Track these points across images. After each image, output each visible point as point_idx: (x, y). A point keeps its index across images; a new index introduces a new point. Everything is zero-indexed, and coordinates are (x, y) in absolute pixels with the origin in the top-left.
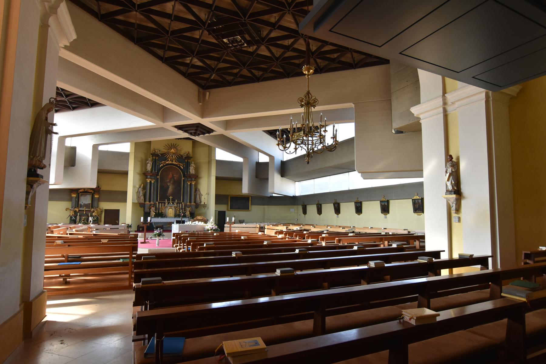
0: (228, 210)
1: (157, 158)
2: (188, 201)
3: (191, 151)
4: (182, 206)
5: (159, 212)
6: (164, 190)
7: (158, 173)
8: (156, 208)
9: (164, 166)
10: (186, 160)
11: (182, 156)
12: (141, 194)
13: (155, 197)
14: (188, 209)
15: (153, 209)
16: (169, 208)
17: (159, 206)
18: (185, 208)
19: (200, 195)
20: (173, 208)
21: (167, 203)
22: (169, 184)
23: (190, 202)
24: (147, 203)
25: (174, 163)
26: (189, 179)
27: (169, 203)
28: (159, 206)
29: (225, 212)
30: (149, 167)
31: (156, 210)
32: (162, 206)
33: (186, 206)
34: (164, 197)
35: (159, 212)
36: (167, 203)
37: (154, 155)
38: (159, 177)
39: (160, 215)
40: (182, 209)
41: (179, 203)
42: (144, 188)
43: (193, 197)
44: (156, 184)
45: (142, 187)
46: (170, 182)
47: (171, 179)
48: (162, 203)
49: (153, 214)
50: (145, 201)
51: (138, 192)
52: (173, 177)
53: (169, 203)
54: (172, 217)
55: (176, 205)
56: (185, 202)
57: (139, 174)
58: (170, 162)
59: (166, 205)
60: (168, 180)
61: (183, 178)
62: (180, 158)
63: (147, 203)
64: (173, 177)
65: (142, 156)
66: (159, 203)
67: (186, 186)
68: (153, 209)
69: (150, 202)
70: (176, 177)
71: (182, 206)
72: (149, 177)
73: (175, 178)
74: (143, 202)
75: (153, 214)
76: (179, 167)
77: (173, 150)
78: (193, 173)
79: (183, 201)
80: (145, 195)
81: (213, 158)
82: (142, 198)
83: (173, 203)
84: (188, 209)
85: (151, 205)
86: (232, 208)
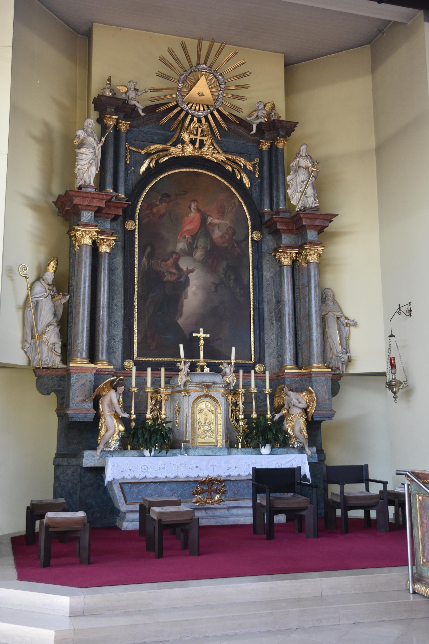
1: (124, 126)
2: (289, 356)
5: (141, 419)
6: (163, 294)
7: (133, 195)
8: (126, 395)
9: (159, 168)
10: (267, 140)
11: (245, 125)
12: (47, 315)
13: (119, 331)
14: (297, 401)
15: (112, 398)
16: (195, 392)
17: (141, 384)
18: (272, 396)
19: (345, 323)
22: (184, 264)
23: (297, 363)
24: (80, 362)
25: (208, 152)
26: (286, 239)
28: (141, 384)
30: (87, 167)
31: (126, 409)
32: (156, 383)
33: (278, 379)
34: (160, 337)
35: (141, 419)
36: (184, 368)
37: (108, 105)
38: (131, 225)
39: (151, 434)
40: (260, 397)
41: (247, 369)
42: (63, 285)
43: (316, 334)
44: (119, 260)
45: (49, 276)
46: (189, 252)
47: (194, 237)
48: (156, 367)
49: (112, 429)
50: (66, 354)
51: (29, 305)
52: (204, 227)
53: (193, 368)
54: (210, 449)
55: (230, 378)
56: (270, 360)
57: (35, 207)
58: (189, 150)
59: (182, 378)
60: (181, 245)
62: (231, 129)
63: (80, 362)
64: (204, 227)
65: (46, 112)
66: (141, 367)
67: (267, 274)
68: (112, 398)
69: (92, 357)
70: (220, 226)
72: (87, 216)
73: (217, 234)
74: (57, 361)
75: (112, 429)
76: (230, 177)
77: (202, 88)
78: (311, 202)
79: (260, 359)
80: (65, 324)
82: (52, 337)
83: (215, 369)
84: (297, 401)
85: (99, 376)
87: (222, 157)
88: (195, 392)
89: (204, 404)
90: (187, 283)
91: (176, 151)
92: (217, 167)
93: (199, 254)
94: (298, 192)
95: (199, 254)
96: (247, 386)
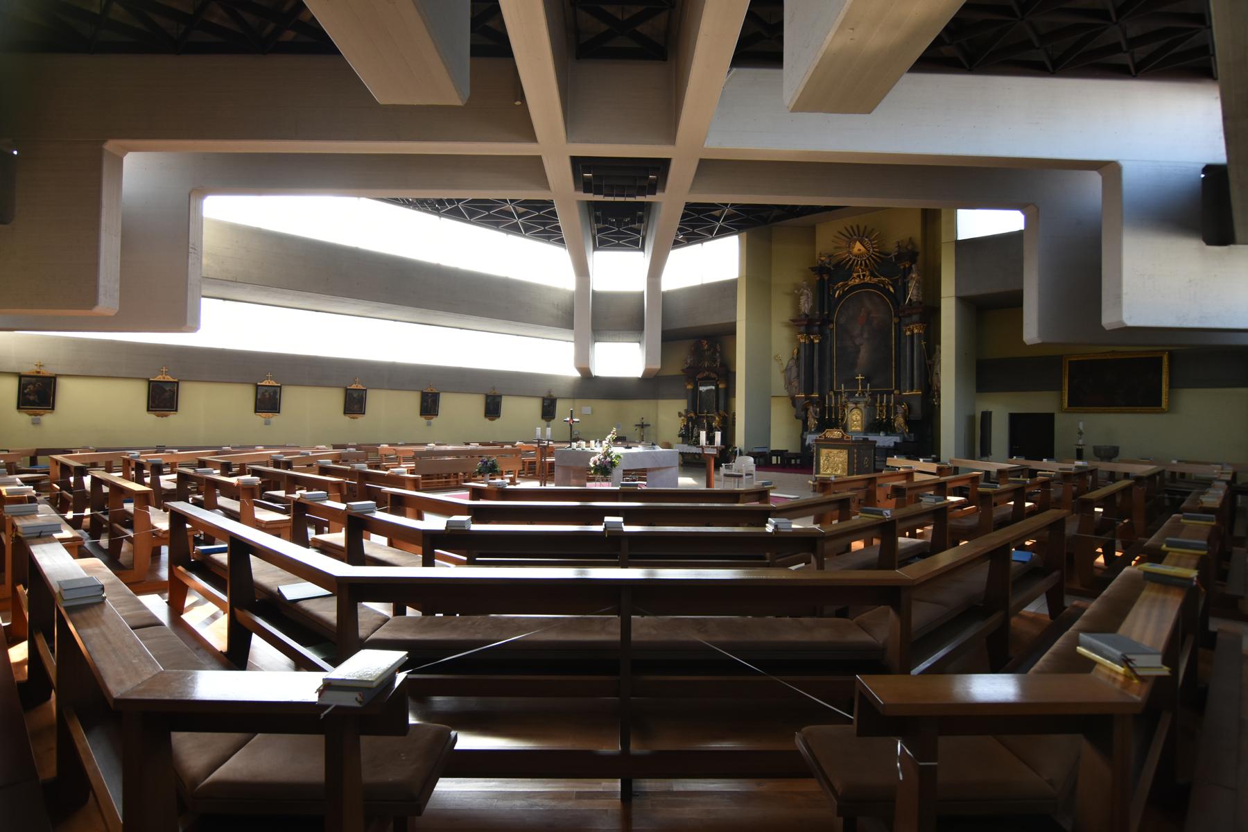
0: (1062, 411)
3: (917, 234)
4: (888, 402)
9: (845, 293)
16: (851, 405)
20: (861, 405)
21: (844, 396)
25: (867, 279)
27: (851, 395)
29: (1052, 415)
36: (844, 396)
49: (812, 422)
57: (787, 325)
58: (857, 281)
61: (895, 320)
71: (888, 402)
75: (812, 422)
79: (898, 387)
81: (944, 238)
86: (1078, 402)
87: (876, 280)
88: (851, 405)
89: (855, 411)
90: (859, 351)
91: (851, 283)
92: (874, 286)
93: (866, 336)
94: (913, 293)
95: (866, 336)
96: (882, 402)
